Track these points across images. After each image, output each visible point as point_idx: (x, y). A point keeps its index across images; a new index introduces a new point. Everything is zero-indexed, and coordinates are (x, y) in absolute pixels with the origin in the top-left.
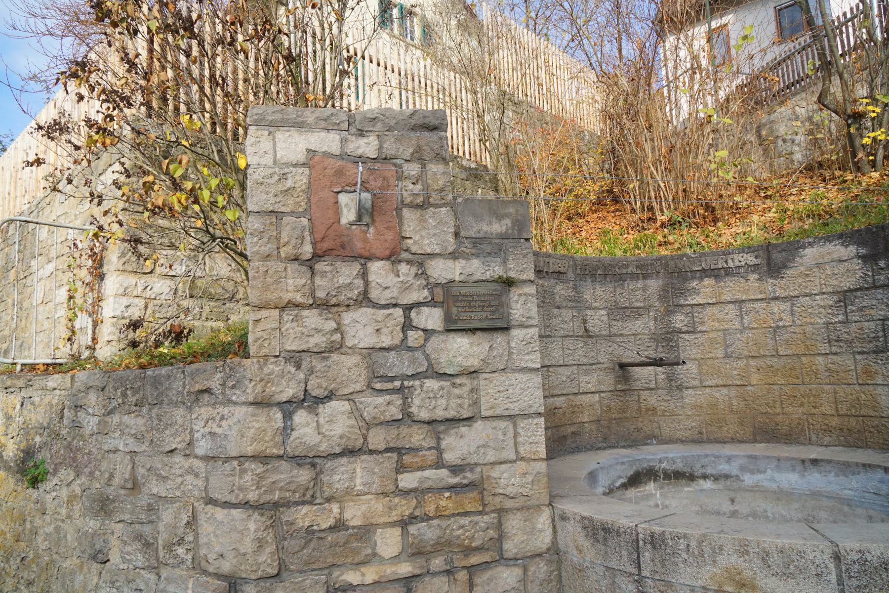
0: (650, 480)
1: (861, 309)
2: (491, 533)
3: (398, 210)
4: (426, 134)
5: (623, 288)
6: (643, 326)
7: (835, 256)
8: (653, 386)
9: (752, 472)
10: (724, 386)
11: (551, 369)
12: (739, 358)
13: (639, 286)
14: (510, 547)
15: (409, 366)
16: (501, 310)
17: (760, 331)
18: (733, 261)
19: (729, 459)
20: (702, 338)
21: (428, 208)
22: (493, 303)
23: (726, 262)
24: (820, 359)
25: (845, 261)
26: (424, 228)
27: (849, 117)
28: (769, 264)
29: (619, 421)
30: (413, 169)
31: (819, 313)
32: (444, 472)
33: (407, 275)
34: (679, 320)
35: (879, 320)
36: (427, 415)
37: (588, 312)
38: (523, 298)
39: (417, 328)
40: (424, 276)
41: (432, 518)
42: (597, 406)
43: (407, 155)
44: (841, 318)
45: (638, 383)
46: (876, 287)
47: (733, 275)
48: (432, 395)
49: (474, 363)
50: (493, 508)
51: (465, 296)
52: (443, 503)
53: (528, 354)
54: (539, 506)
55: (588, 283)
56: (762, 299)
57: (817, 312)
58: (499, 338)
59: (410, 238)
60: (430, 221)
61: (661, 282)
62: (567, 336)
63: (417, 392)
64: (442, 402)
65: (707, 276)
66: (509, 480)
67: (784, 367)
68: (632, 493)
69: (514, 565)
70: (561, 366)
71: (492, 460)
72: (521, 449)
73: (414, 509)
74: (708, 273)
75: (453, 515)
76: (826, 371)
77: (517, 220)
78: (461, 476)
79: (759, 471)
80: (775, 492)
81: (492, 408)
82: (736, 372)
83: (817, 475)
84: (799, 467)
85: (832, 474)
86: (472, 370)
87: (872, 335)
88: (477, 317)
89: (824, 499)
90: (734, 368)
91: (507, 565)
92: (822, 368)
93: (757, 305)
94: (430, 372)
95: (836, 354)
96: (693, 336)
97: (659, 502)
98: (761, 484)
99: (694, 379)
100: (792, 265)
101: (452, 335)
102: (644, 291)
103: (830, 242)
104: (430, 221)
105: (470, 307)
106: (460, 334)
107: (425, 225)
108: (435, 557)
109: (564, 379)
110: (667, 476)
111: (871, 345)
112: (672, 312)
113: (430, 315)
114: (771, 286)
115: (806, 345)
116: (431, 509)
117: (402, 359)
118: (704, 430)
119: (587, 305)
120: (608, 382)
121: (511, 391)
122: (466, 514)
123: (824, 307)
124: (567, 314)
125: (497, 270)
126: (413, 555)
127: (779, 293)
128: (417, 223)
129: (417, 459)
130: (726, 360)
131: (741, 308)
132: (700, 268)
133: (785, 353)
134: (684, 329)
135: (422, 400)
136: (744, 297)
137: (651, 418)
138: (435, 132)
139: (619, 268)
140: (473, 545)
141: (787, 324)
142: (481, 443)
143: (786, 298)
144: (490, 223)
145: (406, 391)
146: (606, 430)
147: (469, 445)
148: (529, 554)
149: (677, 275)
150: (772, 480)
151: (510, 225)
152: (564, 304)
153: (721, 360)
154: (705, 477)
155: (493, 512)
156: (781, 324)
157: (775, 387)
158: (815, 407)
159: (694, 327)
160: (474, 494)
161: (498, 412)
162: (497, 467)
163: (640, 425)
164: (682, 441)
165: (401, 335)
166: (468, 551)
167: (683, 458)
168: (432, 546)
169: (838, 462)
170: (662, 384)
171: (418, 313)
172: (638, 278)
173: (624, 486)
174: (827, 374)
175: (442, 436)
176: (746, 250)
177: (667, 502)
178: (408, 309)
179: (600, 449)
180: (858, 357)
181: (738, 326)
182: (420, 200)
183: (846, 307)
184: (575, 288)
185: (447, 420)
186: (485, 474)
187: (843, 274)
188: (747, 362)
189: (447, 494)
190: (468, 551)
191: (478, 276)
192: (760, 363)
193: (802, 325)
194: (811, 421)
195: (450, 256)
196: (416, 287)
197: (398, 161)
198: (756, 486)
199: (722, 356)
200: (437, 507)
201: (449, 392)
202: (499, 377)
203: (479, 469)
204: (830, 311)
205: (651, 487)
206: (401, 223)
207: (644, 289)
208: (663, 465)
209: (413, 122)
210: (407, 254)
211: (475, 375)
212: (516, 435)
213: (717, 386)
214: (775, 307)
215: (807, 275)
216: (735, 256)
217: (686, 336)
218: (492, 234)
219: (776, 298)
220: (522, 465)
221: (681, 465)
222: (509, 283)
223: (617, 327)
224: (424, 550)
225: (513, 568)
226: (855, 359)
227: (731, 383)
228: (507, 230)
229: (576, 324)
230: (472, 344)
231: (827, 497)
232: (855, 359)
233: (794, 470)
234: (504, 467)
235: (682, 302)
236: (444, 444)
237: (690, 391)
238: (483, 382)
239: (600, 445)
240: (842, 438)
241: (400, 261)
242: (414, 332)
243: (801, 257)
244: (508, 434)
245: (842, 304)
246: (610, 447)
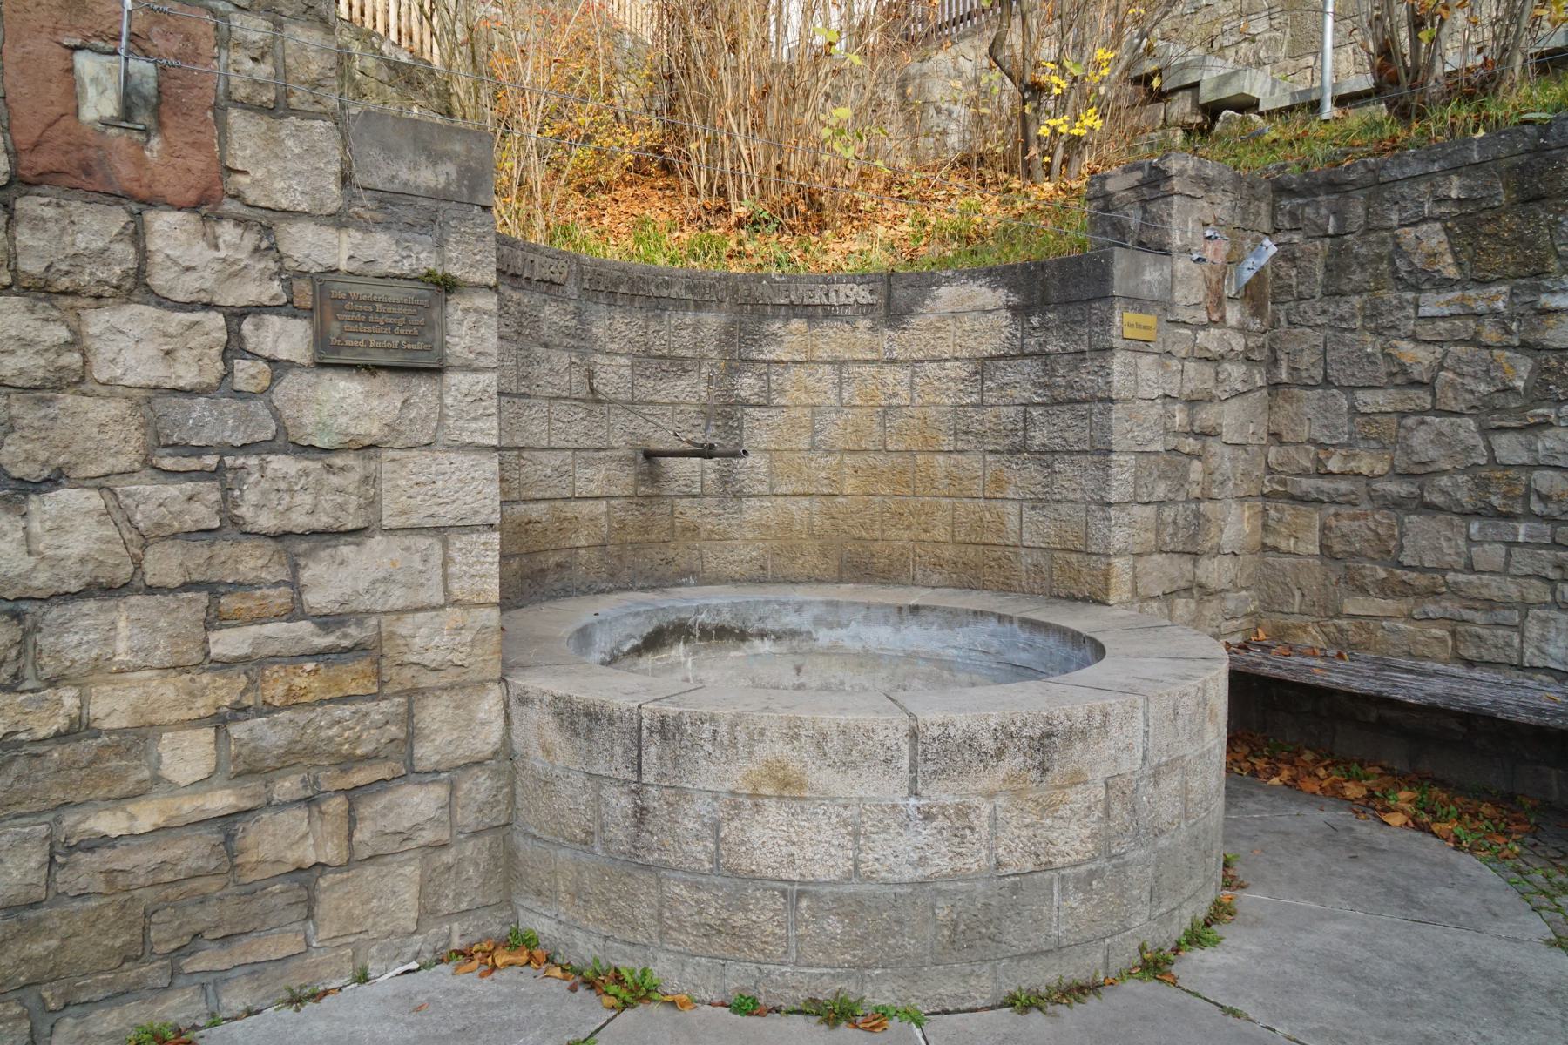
1: (1001, 387)
2: (393, 730)
3: (219, 111)
5: (661, 323)
6: (690, 389)
7: (979, 302)
8: (696, 491)
10: (804, 495)
11: (525, 454)
12: (830, 452)
14: (427, 754)
15: (235, 429)
16: (429, 336)
17: (864, 411)
19: (800, 607)
20: (778, 417)
22: (414, 320)
23: (827, 295)
24: (941, 458)
25: (990, 311)
26: (276, 156)
27: (1027, 87)
28: (888, 305)
29: (637, 546)
32: (304, 627)
33: (237, 247)
34: (747, 385)
37: (599, 359)
38: (472, 317)
39: (255, 356)
40: (273, 253)
42: (603, 521)
44: (975, 398)
45: (673, 485)
46: (1024, 356)
47: (835, 317)
48: (283, 485)
49: (371, 429)
50: (399, 688)
51: (357, 301)
52: (300, 682)
53: (474, 419)
56: (872, 361)
57: (945, 387)
58: (423, 388)
59: (244, 172)
60: (290, 143)
62: (558, 398)
63: (252, 479)
64: (306, 499)
65: (796, 316)
66: (429, 640)
68: (648, 661)
70: (543, 449)
71: (400, 604)
72: (455, 587)
73: (242, 694)
75: (321, 702)
77: (469, 169)
79: (840, 625)
80: (857, 655)
81: (403, 512)
82: (823, 474)
83: (915, 628)
84: (894, 619)
86: (367, 442)
87: (1010, 427)
90: (821, 468)
91: (420, 783)
92: (941, 473)
93: (866, 370)
95: (961, 452)
98: (840, 643)
99: (761, 481)
101: (328, 375)
102: (694, 330)
103: (975, 279)
104: (290, 143)
105: (366, 323)
106: (345, 374)
107: (277, 150)
109: (549, 472)
112: (737, 370)
113: (283, 332)
117: (222, 414)
120: (624, 480)
121: (440, 484)
122: (346, 699)
123: (954, 380)
124: (561, 359)
125: (423, 259)
126: (239, 775)
127: (898, 353)
130: (812, 455)
132: (786, 301)
134: (754, 400)
135: (264, 493)
136: (847, 356)
137: (690, 543)
140: (358, 752)
142: (380, 574)
144: (415, 166)
146: (615, 561)
147: (355, 579)
149: (751, 308)
150: (856, 637)
151: (454, 175)
153: (805, 454)
154: (762, 635)
155: (397, 694)
156: (895, 401)
157: (876, 499)
158: (925, 531)
159: (768, 399)
160: (363, 665)
161: (415, 520)
162: (409, 619)
165: (220, 366)
168: (278, 757)
169: (944, 610)
171: (258, 327)
172: (687, 309)
173: (637, 651)
174: (947, 481)
175: (302, 562)
177: (702, 675)
178: (235, 315)
179: (602, 591)
180: (989, 458)
181: (834, 401)
182: (268, 96)
184: (578, 313)
185: (314, 533)
189: (310, 666)
190: (347, 762)
191: (385, 266)
192: (859, 461)
195: (331, 220)
196: (254, 273)
200: (290, 690)
201: (318, 482)
203: (373, 621)
205: (679, 651)
207: (696, 328)
208: (701, 618)
211: (372, 452)
212: (446, 562)
213: (795, 495)
214: (891, 375)
216: (841, 287)
217: (755, 412)
218: (417, 188)
219: (892, 361)
220: (454, 615)
221: (728, 617)
222: (447, 286)
223: (646, 388)
224: (260, 765)
225: (431, 787)
226: (985, 461)
228: (448, 184)
230: (367, 394)
232: (985, 461)
233: (886, 623)
235: (754, 355)
236: (305, 576)
237: (753, 502)
238: (387, 466)
241: (220, 218)
242: (248, 363)
243: (934, 299)
244: (432, 559)
246: (620, 589)
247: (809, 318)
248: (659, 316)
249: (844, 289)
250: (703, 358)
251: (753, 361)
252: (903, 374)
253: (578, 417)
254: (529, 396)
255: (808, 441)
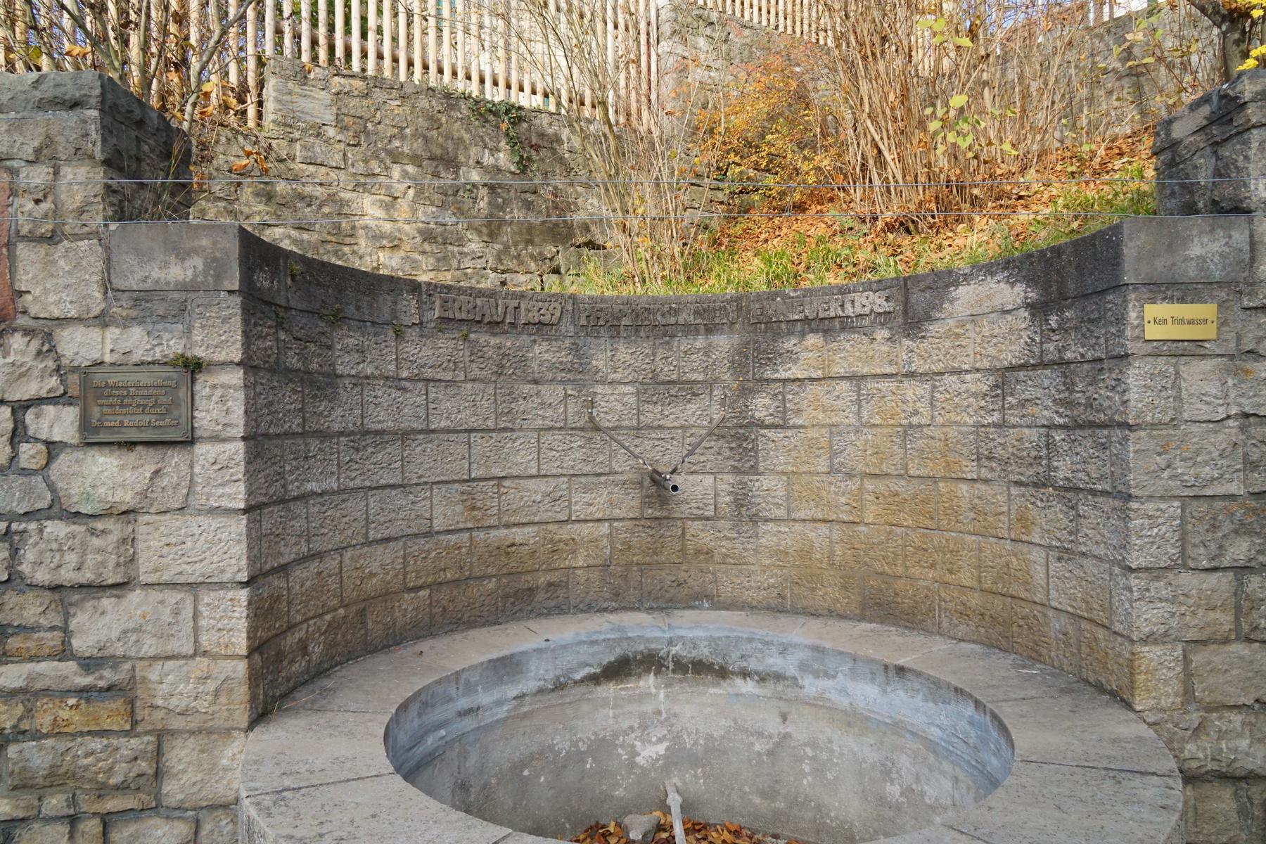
0: (648, 671)
1: (1023, 404)
2: (143, 765)
3: (9, 245)
4: (63, 114)
5: (671, 349)
6: (700, 413)
7: (997, 302)
8: (710, 513)
9: (816, 675)
10: (824, 521)
11: (507, 483)
12: (850, 476)
13: (698, 344)
14: (173, 790)
15: (21, 500)
16: (176, 413)
17: (885, 431)
18: (853, 306)
19: (784, 650)
20: (795, 437)
21: (61, 241)
22: (163, 400)
23: (842, 306)
24: (964, 487)
25: (1008, 312)
26: (52, 275)
27: (1224, 18)
28: (905, 312)
29: (643, 568)
30: (38, 176)
31: (969, 406)
32: (71, 666)
33: (23, 353)
34: (762, 406)
35: (1043, 426)
36: (48, 577)
37: (599, 389)
38: (219, 392)
39: (37, 440)
40: (53, 354)
41: (47, 736)
42: (605, 541)
43: (28, 152)
44: (996, 417)
45: (684, 507)
46: (1043, 365)
47: (852, 329)
48: (54, 546)
49: (126, 498)
50: (150, 727)
51: (115, 387)
52: (65, 714)
53: (222, 485)
54: (228, 731)
55: (602, 341)
56: (892, 375)
57: (962, 406)
58: (175, 458)
59: (28, 292)
60: (62, 263)
61: (736, 339)
62: (551, 429)
63: (31, 541)
64: (72, 558)
65: (812, 331)
66: (172, 688)
67: (915, 496)
68: (609, 690)
69: (179, 818)
70: (532, 477)
71: (152, 652)
72: (204, 639)
73: (20, 720)
74: (814, 325)
75: (81, 734)
76: (971, 510)
77: (214, 260)
78: (97, 675)
79: (827, 675)
80: (845, 712)
81: (156, 570)
82: (843, 500)
83: (902, 693)
84: (880, 678)
85: (920, 696)
86: (124, 508)
87: (1034, 453)
88: (133, 424)
89: (908, 735)
90: (840, 492)
91: (168, 818)
92: (965, 505)
93: (885, 385)
94: (56, 509)
95: (986, 481)
96: (780, 434)
97: (662, 708)
98: (827, 695)
99: (778, 505)
100: (938, 315)
101: (93, 452)
102: (706, 354)
103: (992, 274)
104: (62, 263)
105: (122, 406)
106: (106, 450)
107: (53, 270)
108: (52, 795)
109: (538, 498)
110: (681, 666)
111: (1031, 472)
112: (751, 391)
113: (58, 418)
114: (910, 353)
115: (947, 462)
116: (44, 721)
117: (11, 488)
118: (788, 593)
119: (598, 377)
120: (629, 504)
121: (189, 544)
122: (103, 733)
123: (975, 395)
124: (553, 393)
125: (173, 345)
126: (15, 788)
127: (918, 366)
128: (38, 266)
129: (30, 644)
130: (831, 479)
131: (860, 389)
132: (801, 316)
133: (918, 473)
134: (769, 421)
135: (41, 553)
136: (865, 371)
137: (703, 565)
138: (78, 110)
139: (663, 315)
140: (112, 781)
141: (924, 421)
142: (131, 625)
143: (926, 374)
144: (165, 265)
145: (16, 538)
146: (618, 581)
147: (110, 628)
148: (205, 804)
149: (763, 326)
150: (843, 691)
151: (200, 268)
152: (550, 376)
153: (824, 477)
154: (745, 674)
155: (148, 733)
156: (915, 420)
157: (898, 530)
158: (951, 572)
159: (784, 419)
160: (118, 704)
161: (166, 577)
162: (158, 666)
163: (682, 576)
164: (752, 608)
165: (8, 449)
166: (102, 791)
167: (712, 640)
168: (45, 778)
169: (928, 678)
170: (724, 509)
171: (38, 416)
172: (698, 333)
173: (594, 679)
174: (972, 515)
175: (72, 611)
176: (875, 287)
177: (677, 709)
178: (20, 408)
179: (605, 610)
180: (1015, 491)
181: (852, 420)
182: (46, 228)
183: (1004, 399)
184: (575, 349)
185: (81, 586)
186: (138, 674)
187: (1005, 338)
188: (862, 484)
189: (72, 701)
190: (102, 791)
191: (137, 356)
193: (943, 425)
194: (943, 595)
195: (97, 321)
196: (36, 373)
197: (15, 164)
198: (821, 698)
199: (825, 469)
200: (55, 720)
201: (82, 543)
202: (174, 521)
203: (127, 666)
204: (983, 403)
205: (649, 682)
206: (13, 269)
208: (674, 650)
209: (38, 94)
210: (26, 318)
211: (132, 516)
212: (196, 616)
213: (814, 521)
214: (914, 391)
215: (958, 336)
216: (856, 296)
217: (771, 434)
218: (167, 284)
219: (911, 375)
220: (202, 663)
221: (706, 651)
222: (193, 367)
223: (652, 414)
224: (30, 783)
225: (176, 823)
226: (1009, 495)
227: (834, 517)
228: (195, 276)
229: (572, 408)
230: (122, 467)
231: (912, 733)
232: (1009, 495)
233: (873, 680)
234: (170, 664)
235: (769, 374)
236: (73, 624)
237: (770, 526)
238: (142, 529)
239: (605, 605)
240: (983, 630)
241: (15, 330)
242: (29, 446)
243: (951, 302)
244: (183, 612)
245: (999, 392)
246: (625, 609)
247: (827, 332)
248: (668, 343)
249: (860, 298)
250: (716, 380)
251: (767, 380)
252: (922, 389)
253: (575, 445)
254: (512, 430)
255: (827, 463)
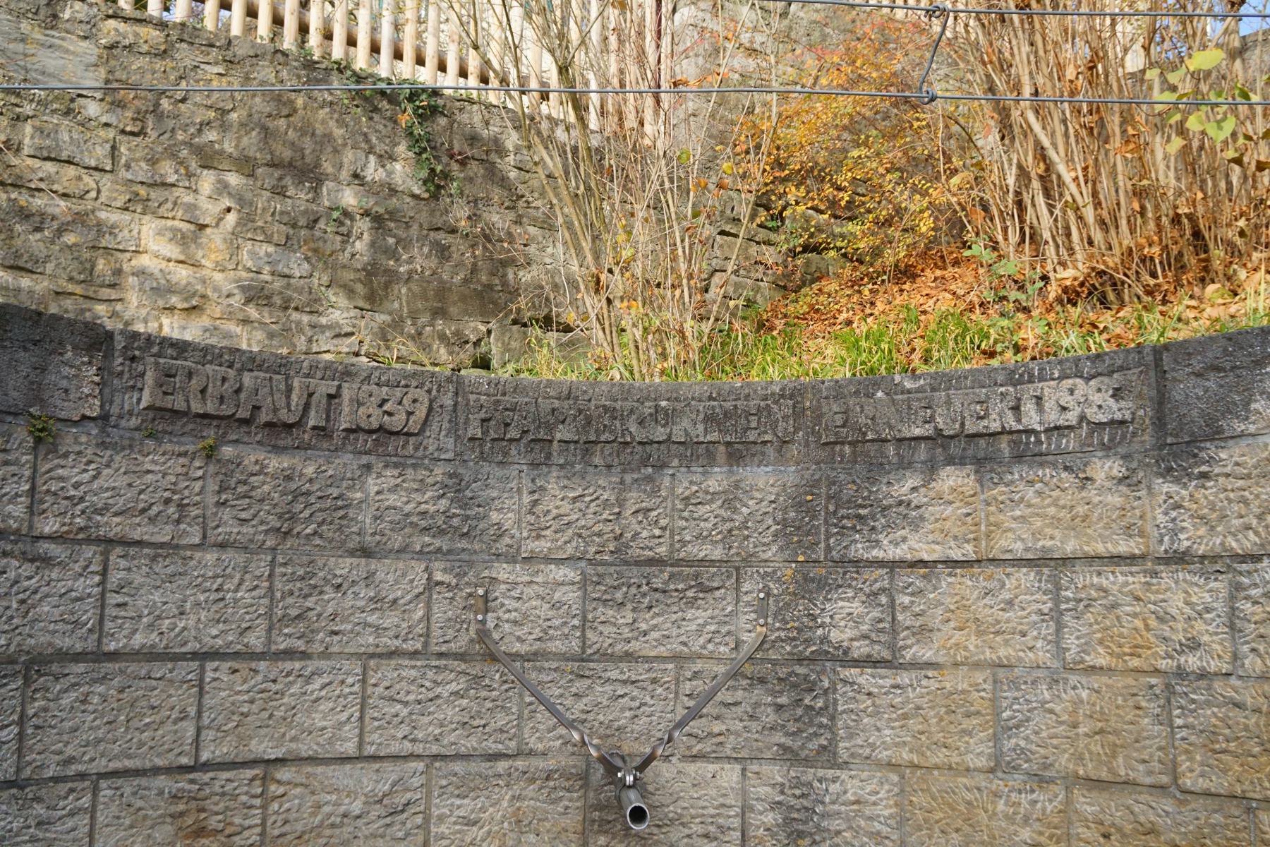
5: (656, 491)
11: (284, 774)
12: (1041, 780)
13: (713, 484)
17: (1120, 682)
20: (918, 689)
23: (1016, 409)
28: (1160, 422)
34: (845, 617)
37: (503, 571)
47: (1039, 458)
55: (513, 471)
56: (1131, 559)
61: (791, 475)
65: (950, 461)
74: (955, 448)
93: (1114, 580)
100: (1240, 427)
102: (729, 504)
109: (357, 807)
112: (822, 584)
114: (1172, 510)
119: (501, 546)
124: (401, 578)
127: (1192, 537)
130: (997, 784)
131: (1058, 588)
132: (928, 430)
133: (1202, 784)
134: (860, 649)
136: (1070, 547)
139: (641, 423)
141: (1213, 666)
143: (1215, 558)
149: (851, 453)
152: (397, 541)
153: (981, 781)
156: (1192, 662)
159: (892, 647)
172: (711, 459)
176: (1087, 368)
181: (1043, 654)
184: (456, 487)
188: (1068, 801)
192: (1114, 809)
199: (982, 762)
207: (730, 501)
214: (1182, 594)
216: (1047, 388)
217: (864, 678)
219: (1179, 559)
223: (613, 626)
235: (859, 550)
247: (980, 463)
248: (649, 479)
249: (1055, 393)
250: (748, 560)
251: (856, 562)
252: (1209, 592)
253: (444, 691)
254: (305, 656)
255: (987, 748)
